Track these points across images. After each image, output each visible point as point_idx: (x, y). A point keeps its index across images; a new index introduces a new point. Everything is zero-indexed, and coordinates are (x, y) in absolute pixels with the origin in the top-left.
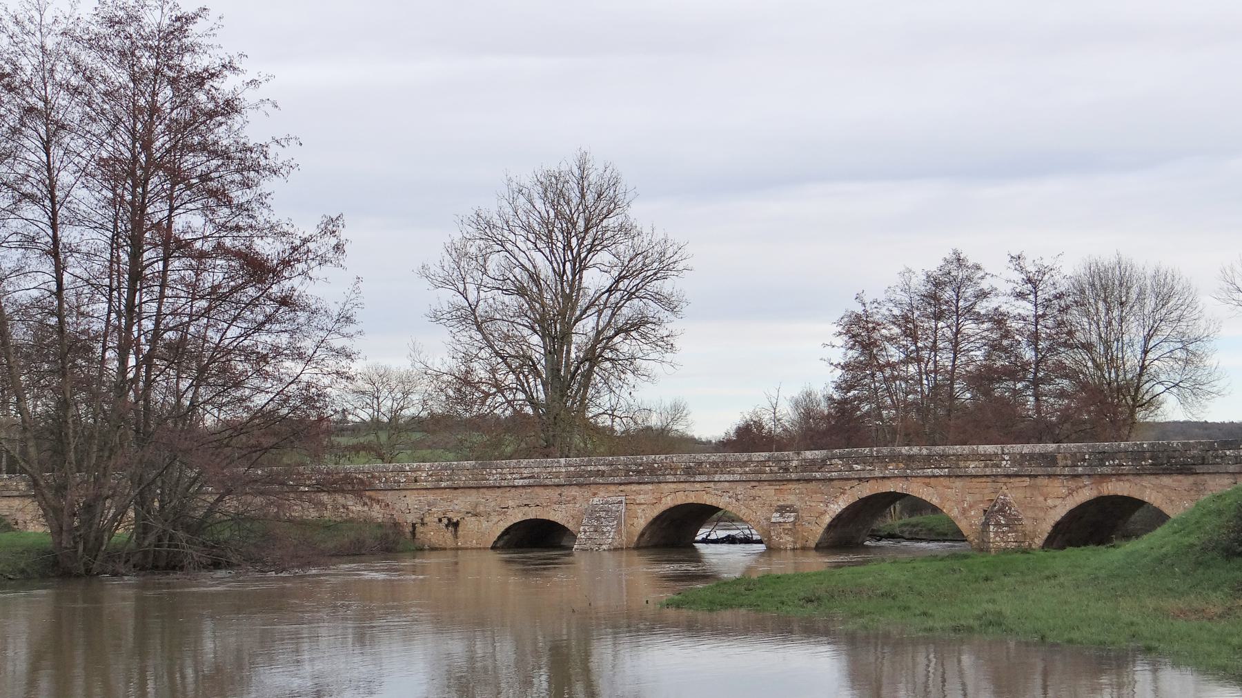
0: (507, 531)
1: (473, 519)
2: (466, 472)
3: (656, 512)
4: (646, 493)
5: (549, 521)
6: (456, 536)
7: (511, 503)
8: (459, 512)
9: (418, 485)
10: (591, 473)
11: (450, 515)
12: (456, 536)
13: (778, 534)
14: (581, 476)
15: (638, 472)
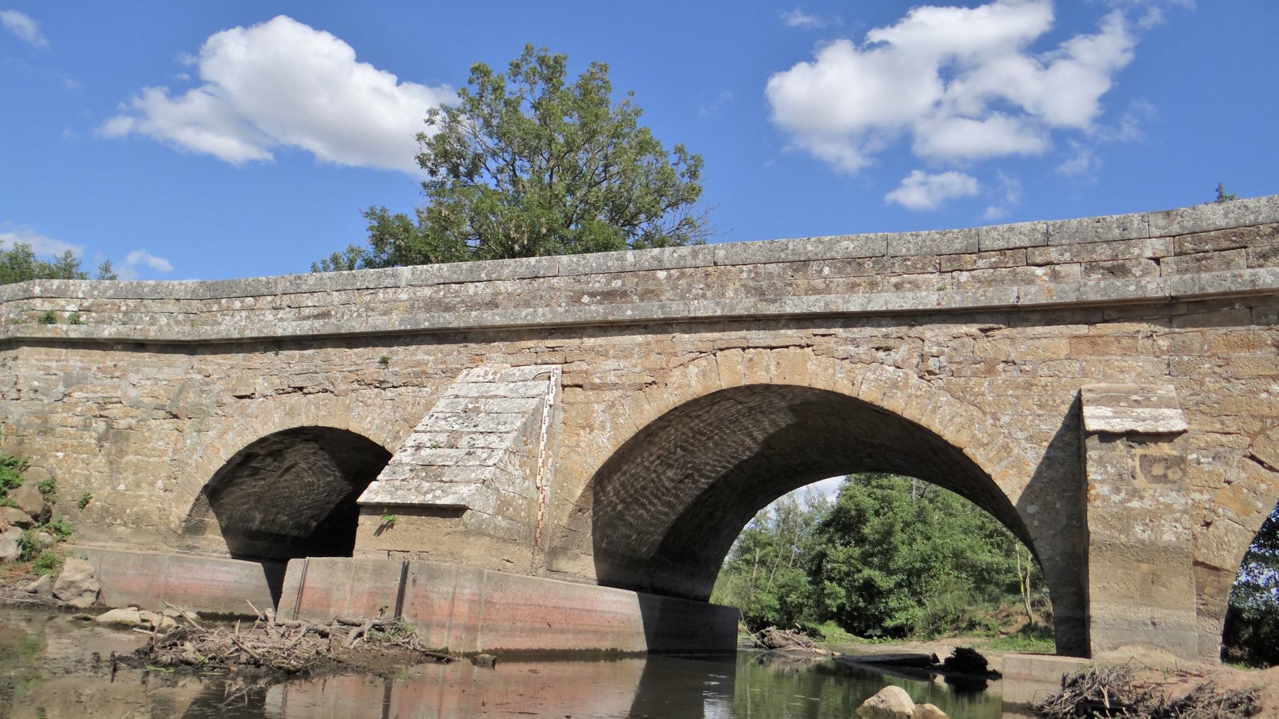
0: (245, 462)
1: (169, 424)
2: (172, 307)
3: (650, 411)
4: (625, 354)
5: (347, 431)
6: (114, 465)
7: (261, 385)
8: (136, 405)
9: (49, 331)
10: (473, 305)
11: (114, 410)
12: (114, 465)
13: (1120, 480)
14: (448, 309)
15: (609, 295)
